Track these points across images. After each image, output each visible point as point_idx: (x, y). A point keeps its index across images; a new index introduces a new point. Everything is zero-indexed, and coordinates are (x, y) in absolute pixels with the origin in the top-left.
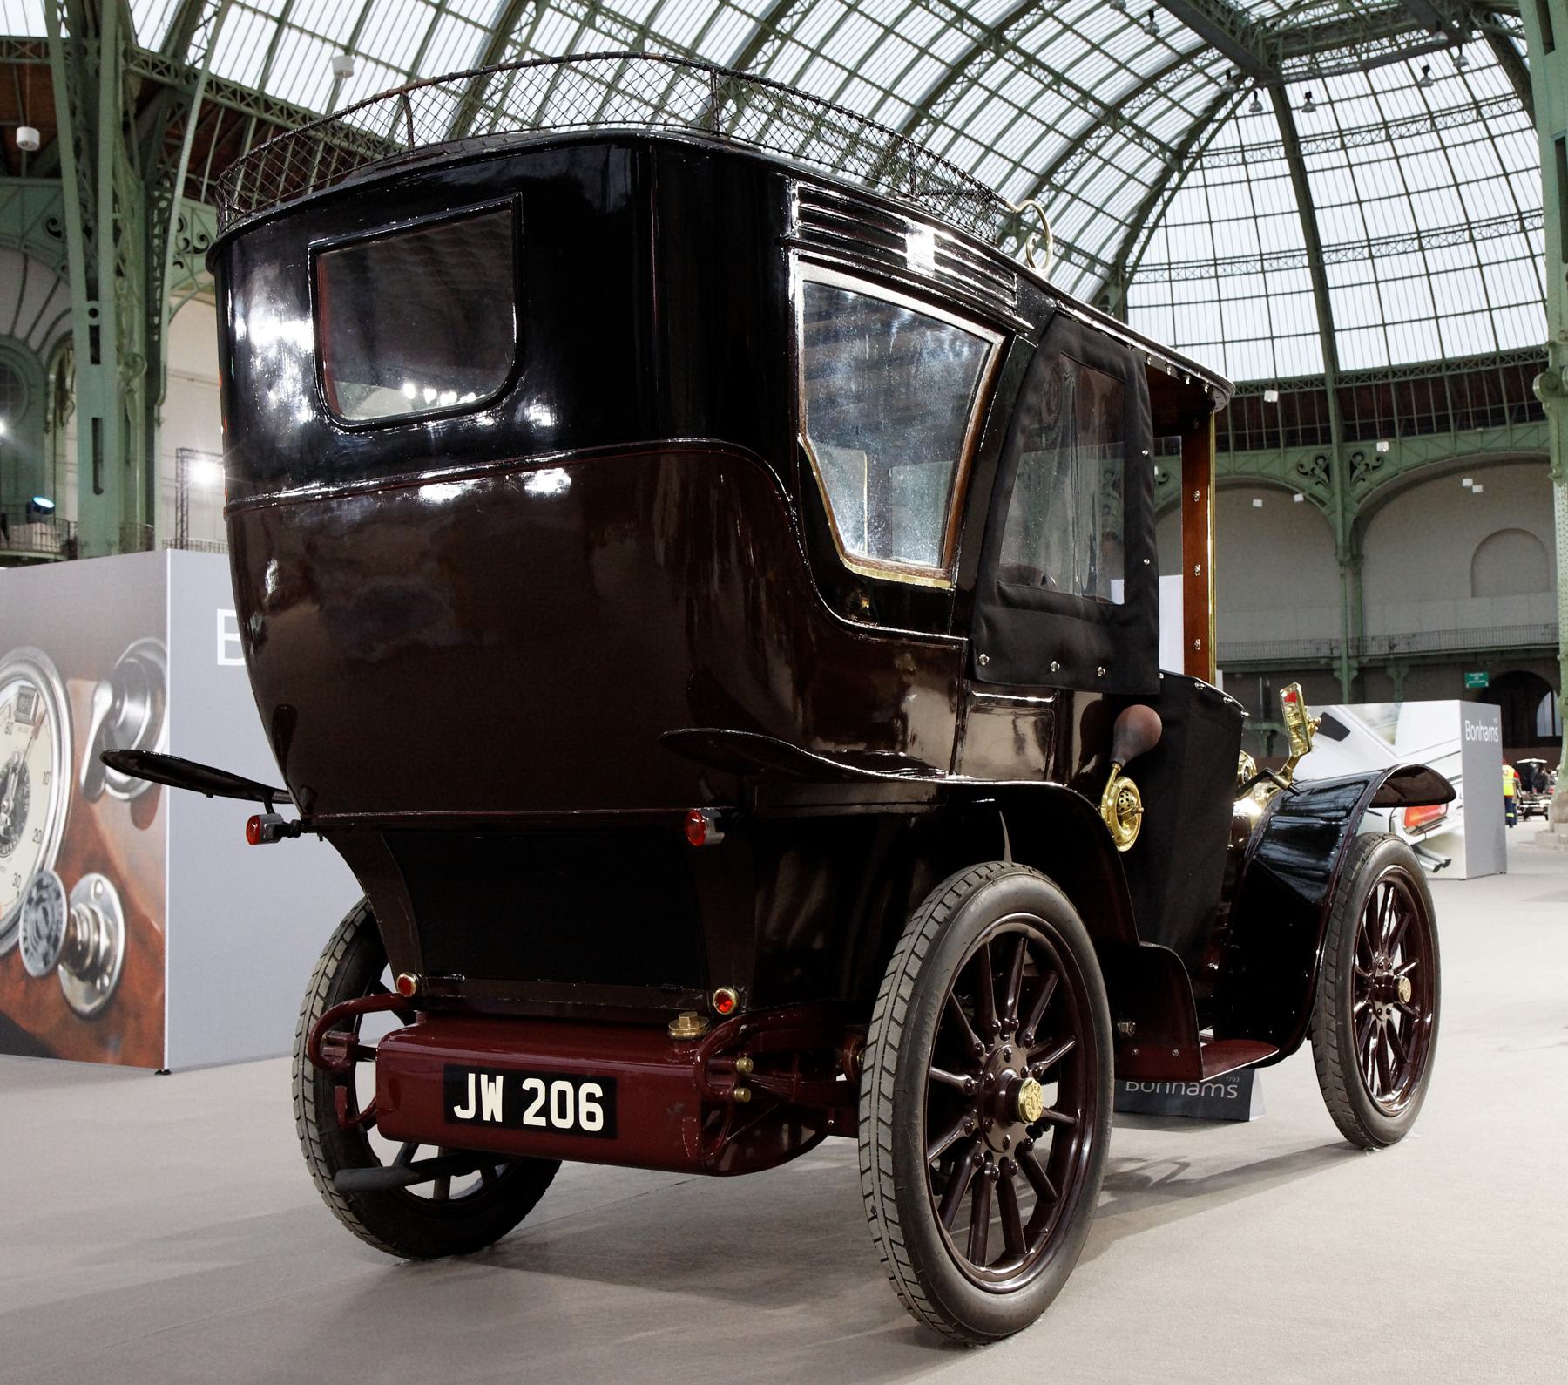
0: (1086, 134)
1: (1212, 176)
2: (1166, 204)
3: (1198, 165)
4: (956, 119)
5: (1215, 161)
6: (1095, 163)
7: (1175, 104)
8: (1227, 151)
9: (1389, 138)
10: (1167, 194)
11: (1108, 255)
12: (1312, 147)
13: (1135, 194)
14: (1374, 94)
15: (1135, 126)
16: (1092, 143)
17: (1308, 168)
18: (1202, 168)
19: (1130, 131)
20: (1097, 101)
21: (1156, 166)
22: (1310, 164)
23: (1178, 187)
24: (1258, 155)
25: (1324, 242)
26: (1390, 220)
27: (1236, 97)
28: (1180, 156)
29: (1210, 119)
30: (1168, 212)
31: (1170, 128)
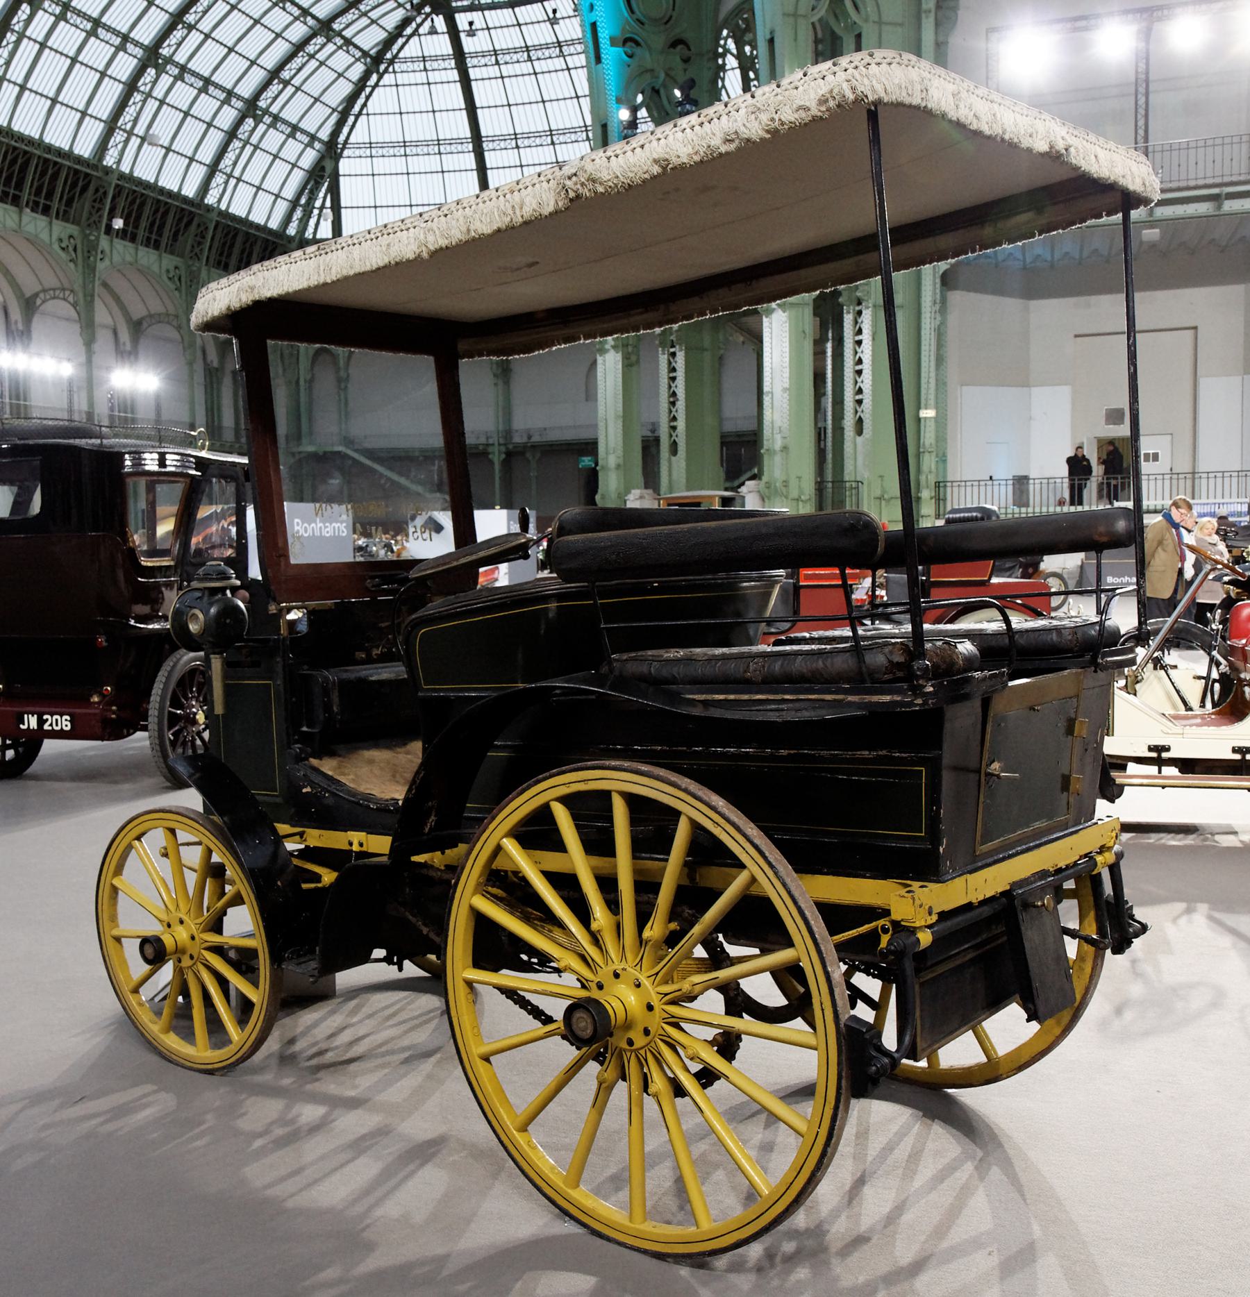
0: (306, 41)
1: (401, 78)
2: (368, 98)
3: (391, 69)
4: (205, 25)
5: (404, 67)
6: (313, 64)
7: (373, 22)
8: (413, 60)
9: (530, 59)
10: (368, 90)
11: (324, 135)
12: (475, 61)
13: (343, 89)
14: (519, 25)
15: (343, 37)
16: (311, 49)
17: (472, 77)
18: (394, 72)
19: (339, 41)
20: (314, 17)
21: (357, 71)
22: (473, 73)
23: (377, 85)
24: (435, 65)
25: (483, 133)
26: (529, 120)
27: (419, 20)
28: (378, 61)
29: (400, 35)
30: (369, 103)
31: (370, 39)
